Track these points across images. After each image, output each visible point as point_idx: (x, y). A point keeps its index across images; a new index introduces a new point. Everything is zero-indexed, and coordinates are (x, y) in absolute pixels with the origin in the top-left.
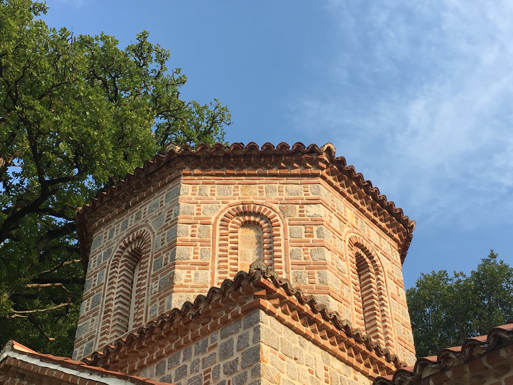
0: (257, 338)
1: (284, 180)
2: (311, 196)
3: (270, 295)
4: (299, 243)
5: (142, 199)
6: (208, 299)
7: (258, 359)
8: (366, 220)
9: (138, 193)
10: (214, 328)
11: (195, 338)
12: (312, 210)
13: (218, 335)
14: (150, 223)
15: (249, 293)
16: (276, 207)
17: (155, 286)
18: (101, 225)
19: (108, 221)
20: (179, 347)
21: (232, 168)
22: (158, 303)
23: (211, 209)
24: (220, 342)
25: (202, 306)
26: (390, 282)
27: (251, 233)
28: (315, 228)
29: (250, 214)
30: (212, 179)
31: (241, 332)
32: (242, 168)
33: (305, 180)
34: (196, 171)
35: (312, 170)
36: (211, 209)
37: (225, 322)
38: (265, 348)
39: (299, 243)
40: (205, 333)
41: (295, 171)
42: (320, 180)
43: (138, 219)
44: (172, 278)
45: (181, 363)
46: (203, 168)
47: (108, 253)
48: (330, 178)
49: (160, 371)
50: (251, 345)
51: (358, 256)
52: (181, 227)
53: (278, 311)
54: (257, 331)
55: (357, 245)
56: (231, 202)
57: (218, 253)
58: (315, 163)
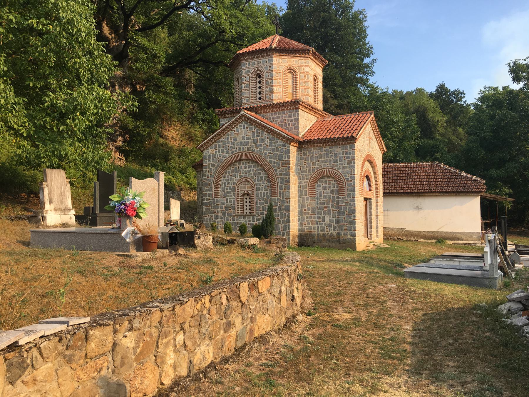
0: (298, 116)
1: (300, 58)
2: (306, 64)
3: (301, 105)
4: (302, 80)
5: (259, 57)
6: (286, 103)
7: (298, 121)
8: (317, 65)
9: (257, 55)
10: (287, 109)
11: (282, 110)
12: (307, 69)
13: (288, 111)
14: (263, 67)
15: (297, 104)
16: (297, 67)
17: (267, 90)
18: (244, 59)
19: (247, 59)
20: (277, 111)
21: (286, 54)
22: (269, 95)
23: (281, 68)
24: (288, 113)
25: (284, 104)
26: (320, 83)
27: (290, 75)
28: (307, 75)
29: (290, 69)
30: (281, 57)
31: (294, 113)
32: (289, 53)
33: (305, 58)
34: (277, 54)
35: (307, 55)
36: (281, 68)
37: (290, 109)
38: (300, 118)
39: (302, 80)
40: (284, 110)
41: (303, 56)
42: (309, 59)
43: (258, 63)
44: (273, 89)
45: (278, 115)
46: (279, 53)
47: (249, 71)
48: (311, 57)
49: (272, 115)
50: (297, 117)
51: (314, 79)
52: (274, 73)
53: (302, 108)
54: (298, 114)
55: (315, 76)
56: (286, 65)
57: (283, 82)
58: (308, 54)
